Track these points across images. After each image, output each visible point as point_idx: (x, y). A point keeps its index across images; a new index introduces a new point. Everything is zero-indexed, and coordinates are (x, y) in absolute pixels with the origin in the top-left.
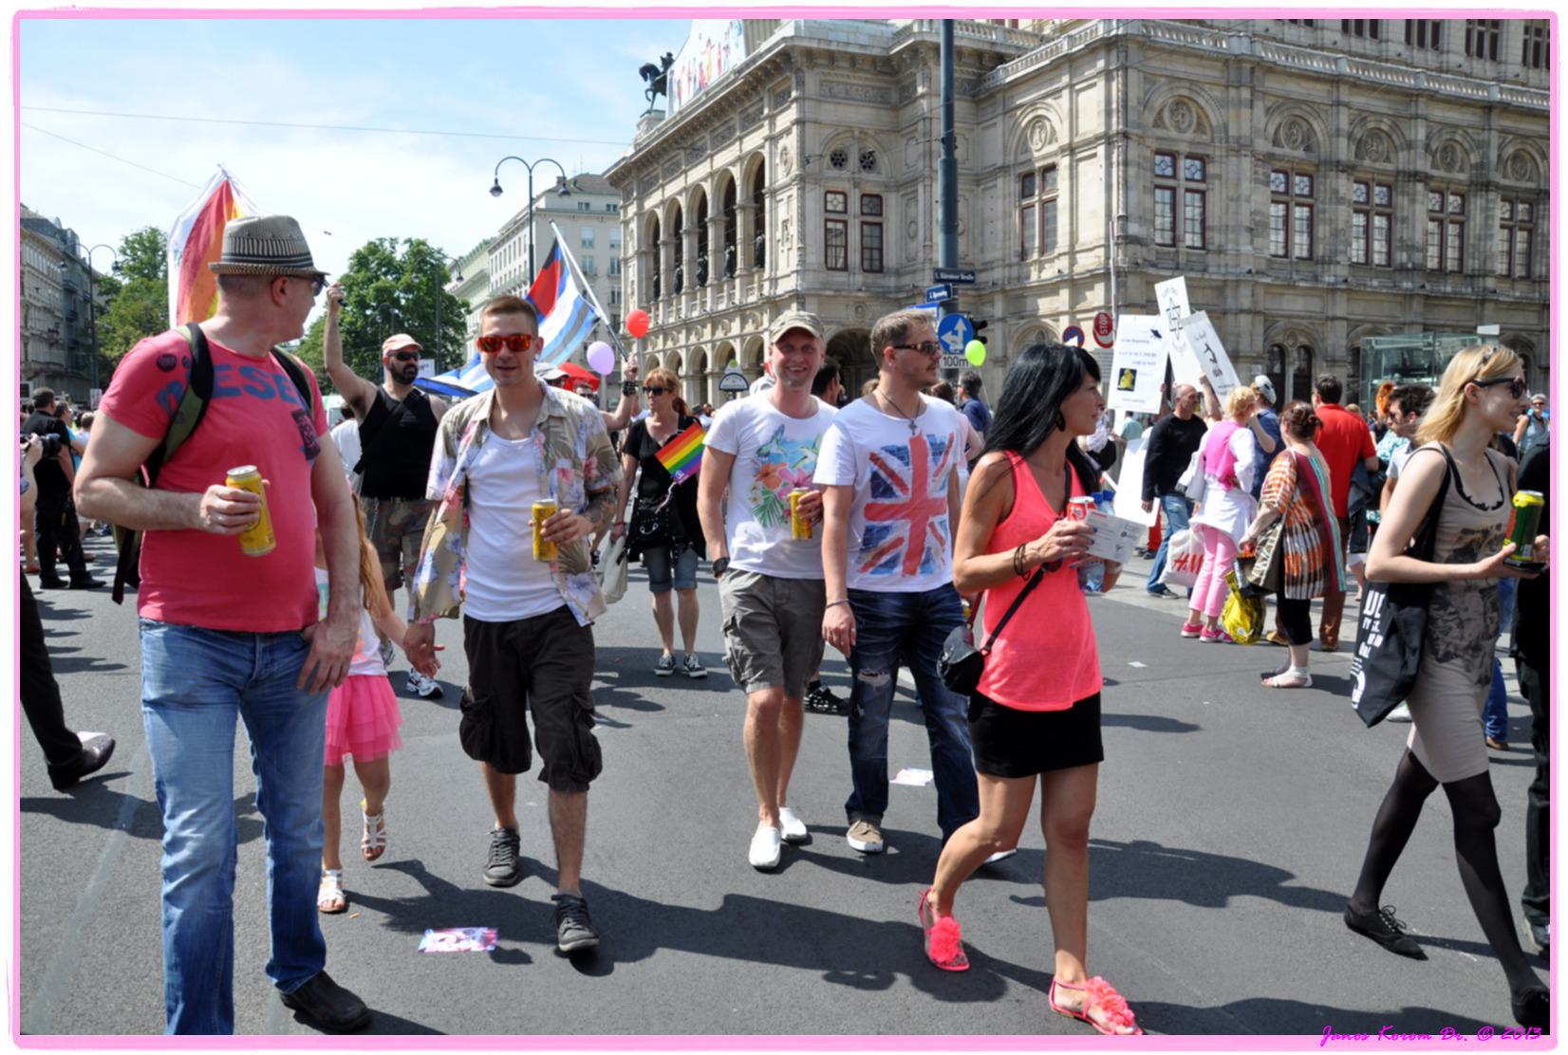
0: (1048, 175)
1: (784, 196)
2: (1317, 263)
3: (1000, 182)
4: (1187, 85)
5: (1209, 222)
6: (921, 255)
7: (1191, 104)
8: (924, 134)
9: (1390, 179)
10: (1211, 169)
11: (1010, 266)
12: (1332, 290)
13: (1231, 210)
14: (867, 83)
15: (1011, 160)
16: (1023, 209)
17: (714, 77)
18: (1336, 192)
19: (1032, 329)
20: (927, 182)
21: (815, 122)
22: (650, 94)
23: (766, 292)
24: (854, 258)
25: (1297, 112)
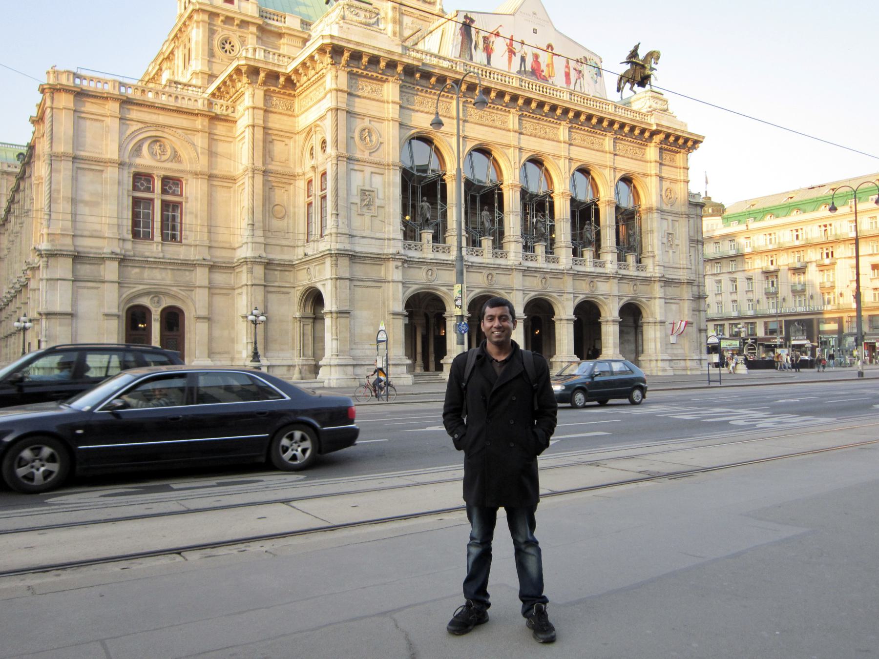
1: (670, 218)
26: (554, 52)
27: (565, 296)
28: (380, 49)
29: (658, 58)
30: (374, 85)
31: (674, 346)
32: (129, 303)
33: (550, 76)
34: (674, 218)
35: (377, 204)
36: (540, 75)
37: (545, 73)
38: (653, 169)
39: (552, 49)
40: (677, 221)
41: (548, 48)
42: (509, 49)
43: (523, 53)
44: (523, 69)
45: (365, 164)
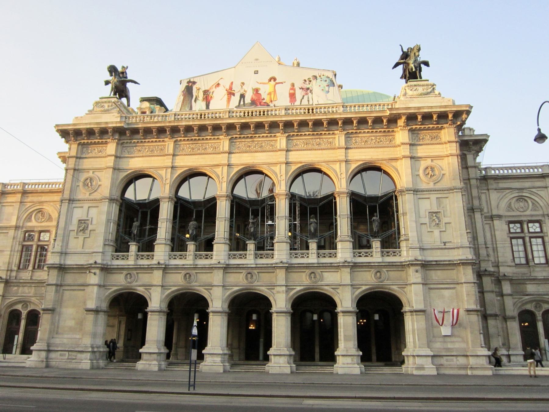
1: (433, 197)
3: (496, 222)
15: (501, 213)
19: (531, 302)
26: (277, 81)
27: (278, 289)
28: (90, 124)
29: (419, 50)
30: (100, 147)
31: (448, 339)
32: (10, 308)
33: (271, 101)
34: (439, 196)
36: (260, 103)
37: (267, 100)
38: (405, 151)
39: (275, 79)
40: (447, 198)
41: (270, 80)
42: (228, 92)
43: (242, 92)
44: (242, 103)
45: (85, 202)
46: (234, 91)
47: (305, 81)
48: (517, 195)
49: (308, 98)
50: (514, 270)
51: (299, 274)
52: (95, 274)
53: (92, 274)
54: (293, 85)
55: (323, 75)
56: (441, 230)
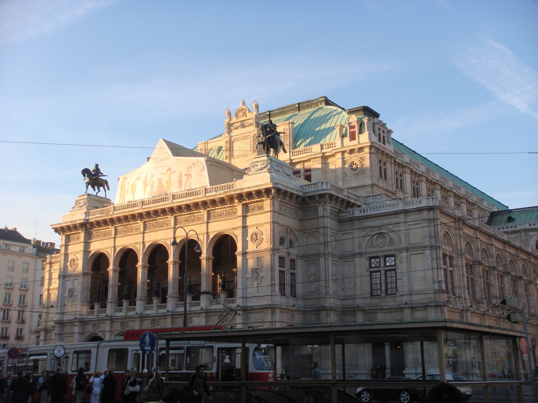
0: (388, 259)
2: (477, 303)
3: (357, 260)
4: (447, 227)
5: (456, 284)
6: (323, 290)
7: (447, 235)
8: (324, 235)
9: (487, 269)
10: (455, 262)
11: (365, 298)
12: (484, 314)
13: (461, 280)
14: (292, 207)
15: (363, 250)
16: (371, 272)
17: (175, 189)
18: (480, 273)
20: (327, 257)
21: (277, 223)
22: (87, 184)
23: (239, 302)
24: (288, 289)
25: (468, 241)
26: (172, 171)
28: (67, 222)
35: (74, 295)
41: (168, 171)
44: (152, 192)
46: (148, 182)
47: (188, 168)
48: (377, 232)
49: (189, 183)
50: (369, 301)
51: (179, 319)
52: (77, 326)
53: (75, 326)
54: (181, 173)
55: (199, 162)
56: (258, 282)
